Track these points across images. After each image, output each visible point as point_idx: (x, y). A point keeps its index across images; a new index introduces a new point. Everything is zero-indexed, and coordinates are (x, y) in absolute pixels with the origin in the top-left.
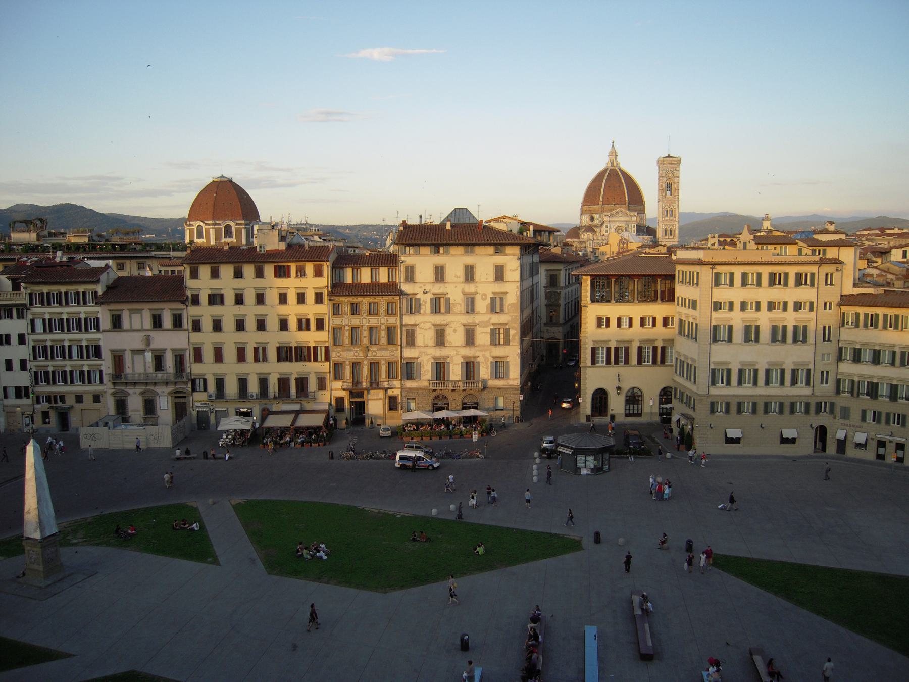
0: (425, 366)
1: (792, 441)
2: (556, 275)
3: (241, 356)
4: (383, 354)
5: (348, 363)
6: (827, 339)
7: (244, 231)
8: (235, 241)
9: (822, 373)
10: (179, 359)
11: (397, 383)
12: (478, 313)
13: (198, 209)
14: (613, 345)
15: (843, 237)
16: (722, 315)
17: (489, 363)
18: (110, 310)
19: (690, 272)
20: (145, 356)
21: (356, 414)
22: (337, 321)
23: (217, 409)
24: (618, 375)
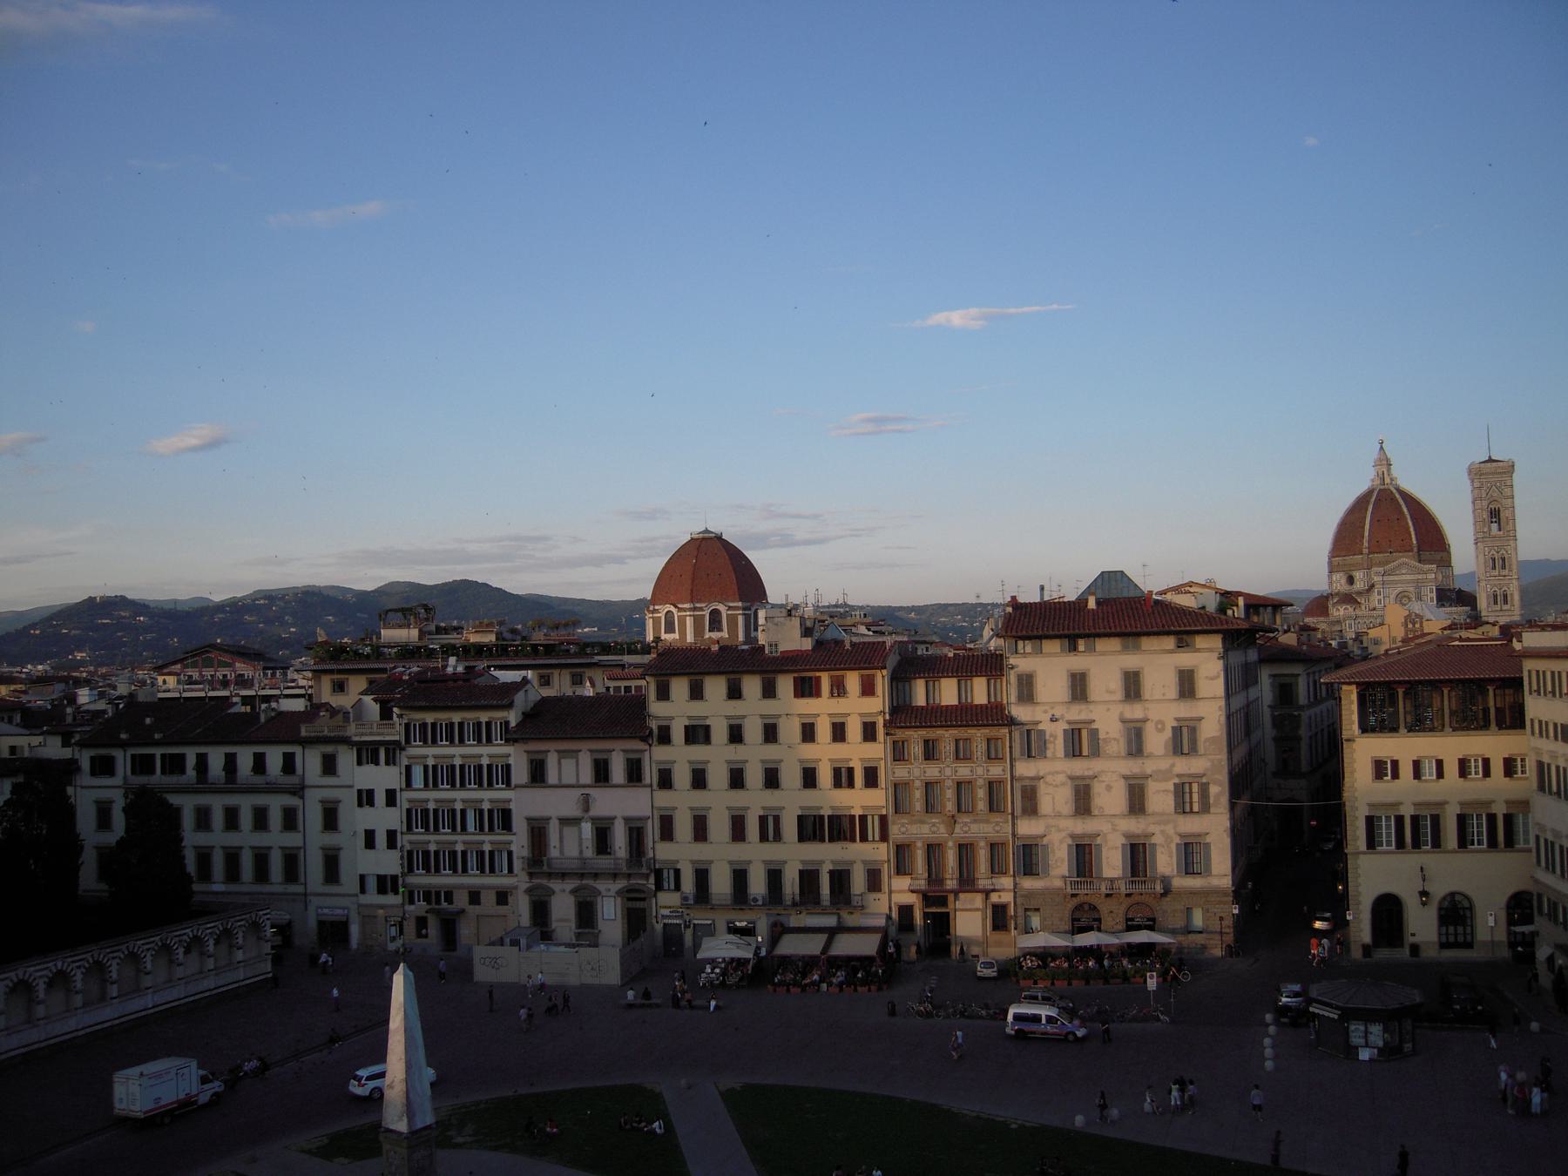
0: (1056, 851)
2: (1291, 685)
3: (738, 830)
4: (981, 829)
5: (919, 844)
7: (741, 620)
10: (636, 834)
11: (1006, 882)
12: (1149, 756)
13: (666, 585)
14: (1407, 811)
17: (1173, 846)
18: (525, 751)
19: (1553, 673)
22: (901, 772)
23: (696, 922)
24: (1422, 868)
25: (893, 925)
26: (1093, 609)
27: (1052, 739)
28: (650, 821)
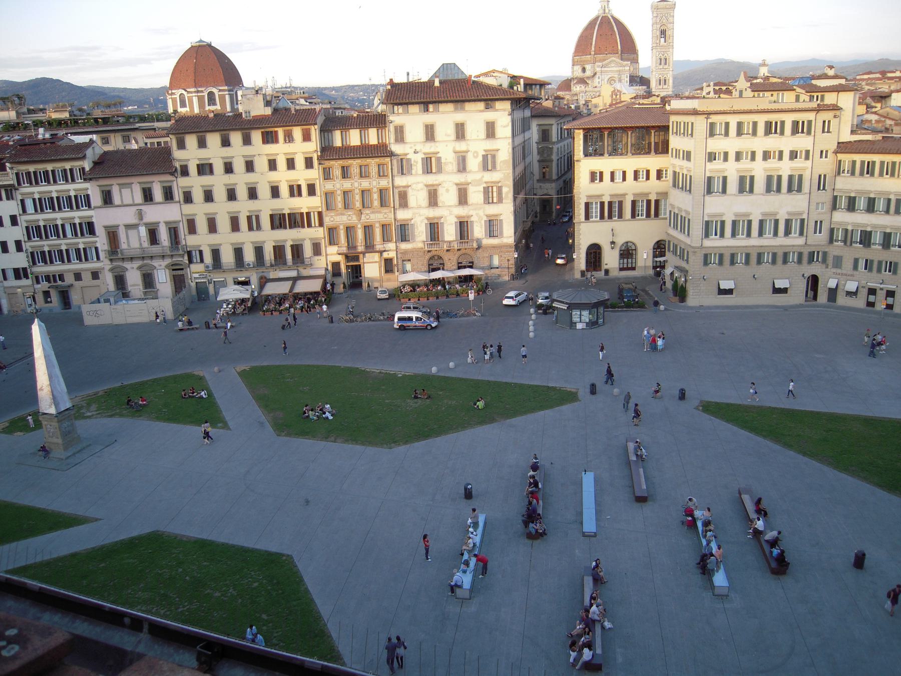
1: (784, 291)
2: (548, 130)
3: (235, 225)
4: (377, 217)
5: (341, 227)
6: (821, 189)
7: (227, 98)
8: (220, 108)
9: (816, 222)
10: (174, 232)
11: (391, 246)
13: (178, 76)
15: (843, 81)
19: (684, 123)
20: (139, 232)
21: (353, 278)
22: (329, 186)
24: (612, 230)
26: (437, 87)
27: (415, 164)
28: (181, 223)
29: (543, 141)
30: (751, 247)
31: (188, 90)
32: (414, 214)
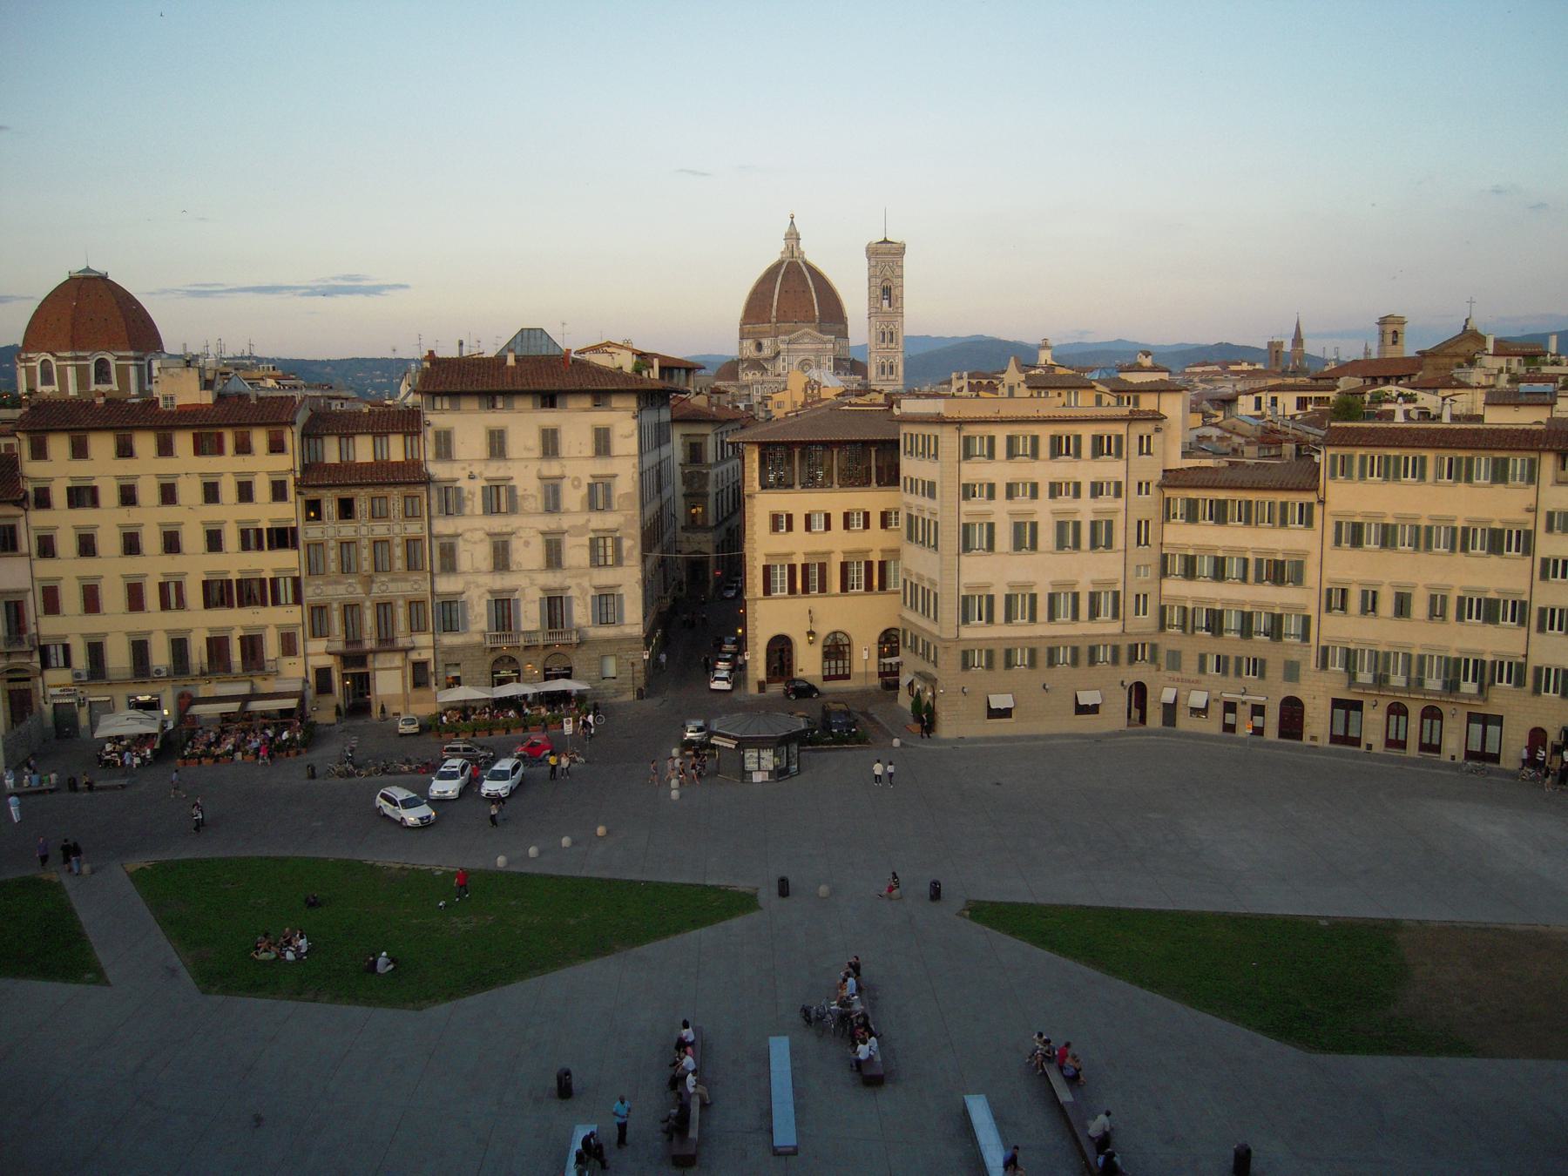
1: (1093, 709)
2: (701, 444)
3: (135, 598)
4: (400, 588)
5: (335, 605)
6: (1143, 542)
7: (133, 372)
8: (117, 389)
9: (1138, 596)
11: (424, 640)
12: (567, 512)
14: (799, 561)
15: (1165, 376)
16: (977, 505)
17: (589, 599)
19: (924, 436)
21: (354, 697)
23: (91, 699)
24: (810, 612)
25: (310, 688)
26: (512, 367)
27: (470, 496)
28: (30, 594)
29: (691, 462)
30: (1036, 638)
31: (59, 354)
32: (467, 583)
